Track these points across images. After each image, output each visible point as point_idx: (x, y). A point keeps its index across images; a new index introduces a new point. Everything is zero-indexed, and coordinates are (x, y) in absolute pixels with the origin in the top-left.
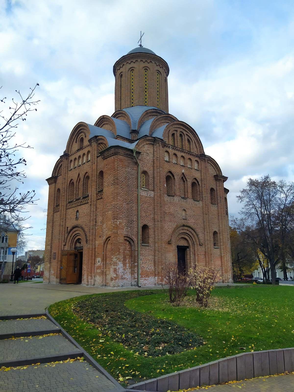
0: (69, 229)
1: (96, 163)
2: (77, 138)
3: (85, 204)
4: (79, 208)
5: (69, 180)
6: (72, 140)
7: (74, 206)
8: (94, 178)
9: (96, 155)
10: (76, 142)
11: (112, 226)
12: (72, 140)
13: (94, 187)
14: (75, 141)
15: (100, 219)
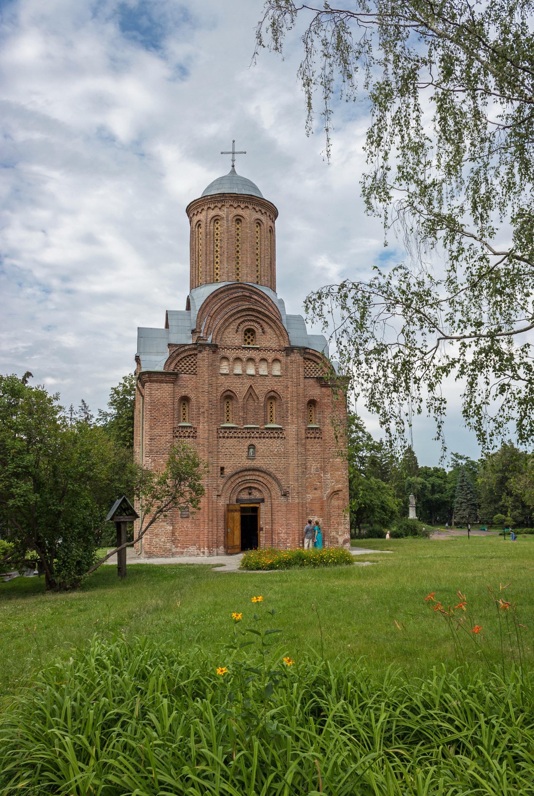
0: (228, 471)
1: (302, 386)
2: (239, 325)
3: (271, 438)
4: (254, 442)
5: (222, 390)
6: (227, 324)
7: (240, 435)
8: (302, 407)
9: (302, 373)
10: (237, 331)
11: (343, 477)
12: (227, 324)
13: (301, 420)
14: (234, 326)
15: (313, 466)
